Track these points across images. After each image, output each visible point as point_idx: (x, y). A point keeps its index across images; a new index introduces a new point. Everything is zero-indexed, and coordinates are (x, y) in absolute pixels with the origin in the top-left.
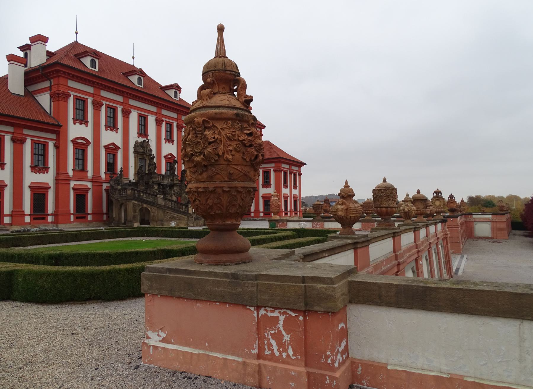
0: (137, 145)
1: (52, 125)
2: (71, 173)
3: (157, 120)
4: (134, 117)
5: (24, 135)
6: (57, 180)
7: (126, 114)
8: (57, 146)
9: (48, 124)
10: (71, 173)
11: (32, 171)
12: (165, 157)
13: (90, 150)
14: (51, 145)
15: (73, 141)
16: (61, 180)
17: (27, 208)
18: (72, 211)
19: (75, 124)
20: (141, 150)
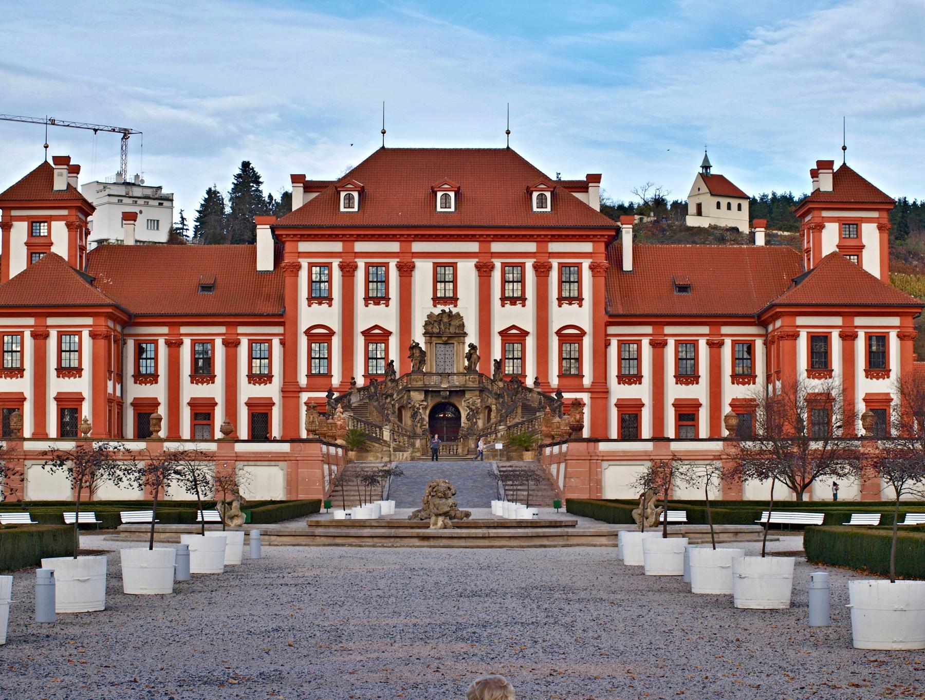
0: (431, 321)
1: (273, 315)
2: (303, 381)
3: (478, 267)
4: (423, 270)
5: (238, 334)
6: (283, 391)
7: (406, 270)
8: (283, 343)
9: (261, 315)
10: (303, 381)
11: (250, 383)
12: (503, 333)
13: (336, 341)
14: (276, 342)
19: (310, 306)
20: (436, 330)
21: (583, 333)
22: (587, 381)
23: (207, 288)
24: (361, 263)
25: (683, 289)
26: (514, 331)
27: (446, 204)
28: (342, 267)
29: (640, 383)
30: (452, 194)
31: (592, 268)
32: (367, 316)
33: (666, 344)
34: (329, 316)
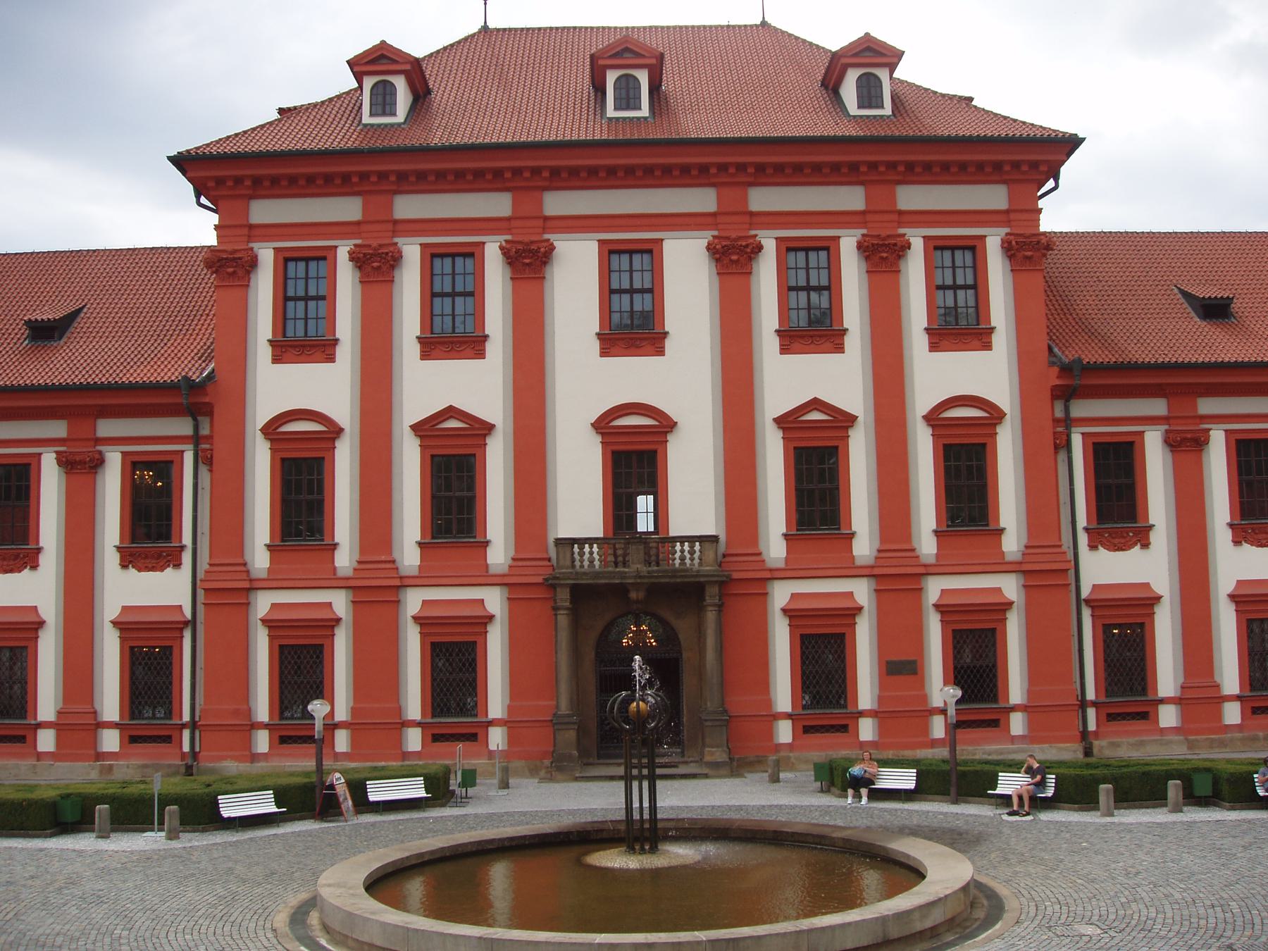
2: (260, 560)
7: (530, 263)
10: (260, 560)
12: (787, 422)
15: (271, 430)
16: (225, 592)
17: (110, 699)
18: (262, 712)
21: (995, 415)
22: (1012, 544)
23: (45, 333)
24: (411, 252)
25: (1215, 310)
26: (815, 416)
27: (627, 98)
28: (359, 259)
29: (1146, 545)
30: (643, 77)
31: (1010, 249)
32: (426, 386)
33: (1207, 442)
34: (328, 388)
